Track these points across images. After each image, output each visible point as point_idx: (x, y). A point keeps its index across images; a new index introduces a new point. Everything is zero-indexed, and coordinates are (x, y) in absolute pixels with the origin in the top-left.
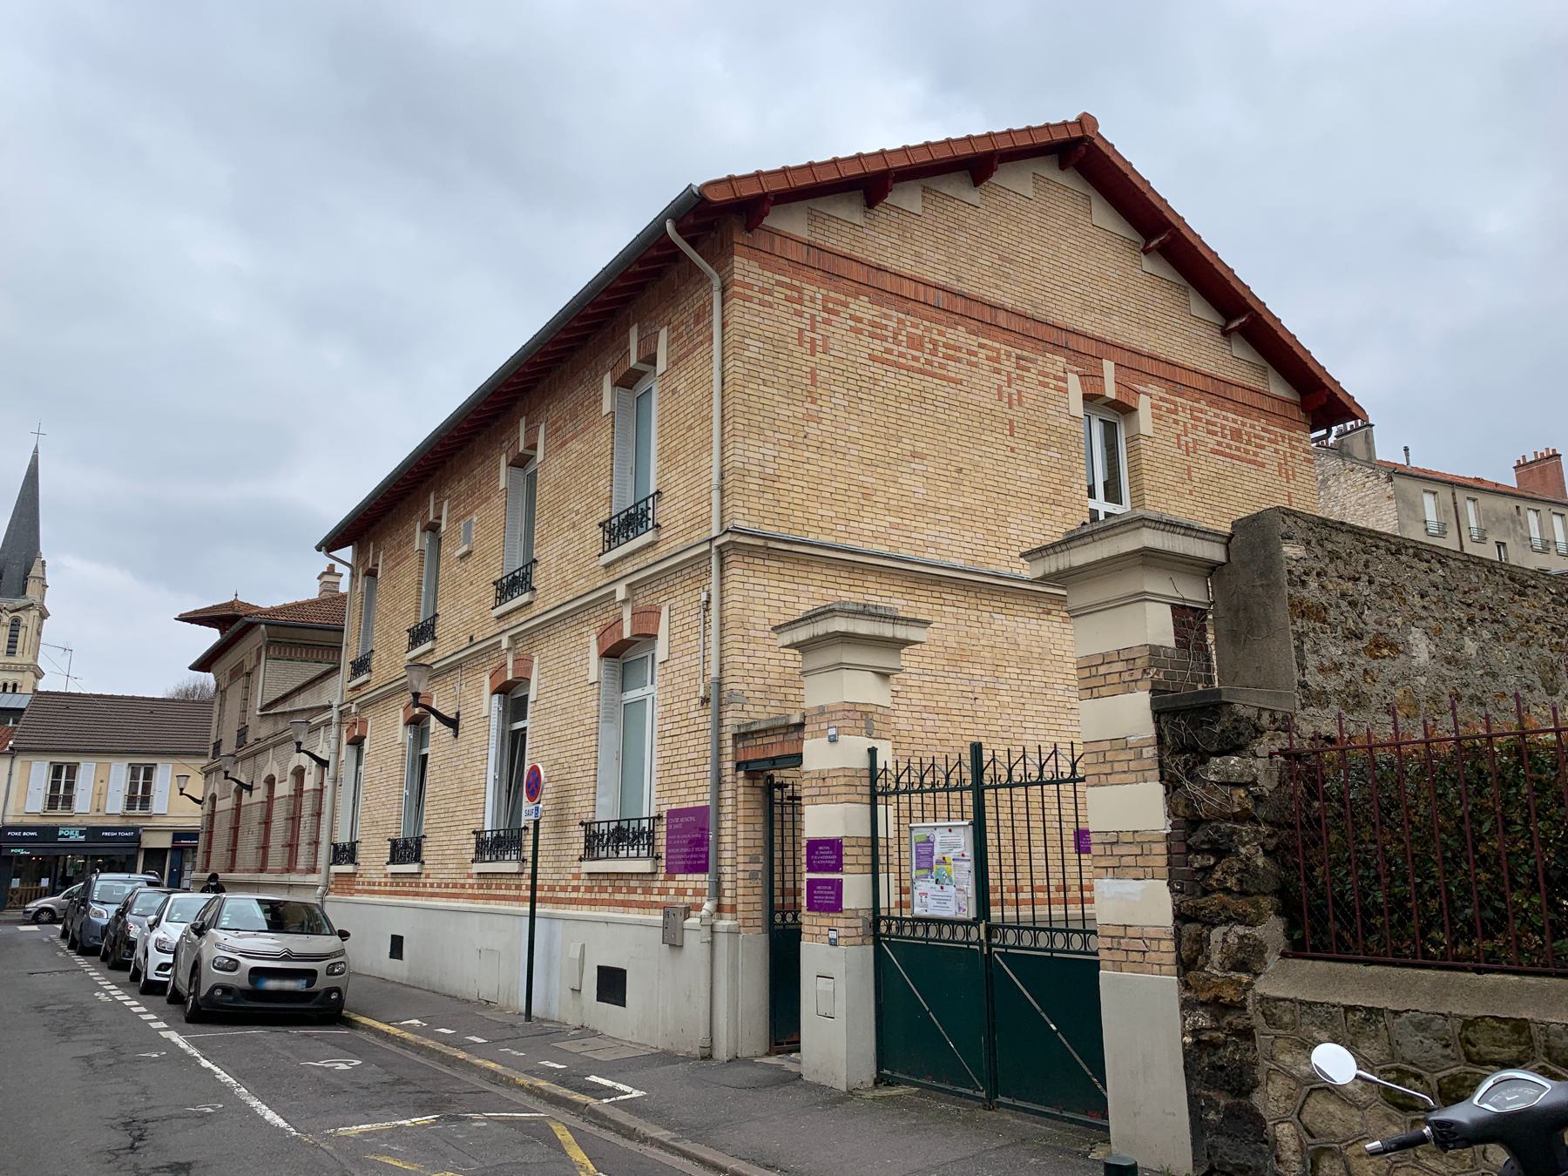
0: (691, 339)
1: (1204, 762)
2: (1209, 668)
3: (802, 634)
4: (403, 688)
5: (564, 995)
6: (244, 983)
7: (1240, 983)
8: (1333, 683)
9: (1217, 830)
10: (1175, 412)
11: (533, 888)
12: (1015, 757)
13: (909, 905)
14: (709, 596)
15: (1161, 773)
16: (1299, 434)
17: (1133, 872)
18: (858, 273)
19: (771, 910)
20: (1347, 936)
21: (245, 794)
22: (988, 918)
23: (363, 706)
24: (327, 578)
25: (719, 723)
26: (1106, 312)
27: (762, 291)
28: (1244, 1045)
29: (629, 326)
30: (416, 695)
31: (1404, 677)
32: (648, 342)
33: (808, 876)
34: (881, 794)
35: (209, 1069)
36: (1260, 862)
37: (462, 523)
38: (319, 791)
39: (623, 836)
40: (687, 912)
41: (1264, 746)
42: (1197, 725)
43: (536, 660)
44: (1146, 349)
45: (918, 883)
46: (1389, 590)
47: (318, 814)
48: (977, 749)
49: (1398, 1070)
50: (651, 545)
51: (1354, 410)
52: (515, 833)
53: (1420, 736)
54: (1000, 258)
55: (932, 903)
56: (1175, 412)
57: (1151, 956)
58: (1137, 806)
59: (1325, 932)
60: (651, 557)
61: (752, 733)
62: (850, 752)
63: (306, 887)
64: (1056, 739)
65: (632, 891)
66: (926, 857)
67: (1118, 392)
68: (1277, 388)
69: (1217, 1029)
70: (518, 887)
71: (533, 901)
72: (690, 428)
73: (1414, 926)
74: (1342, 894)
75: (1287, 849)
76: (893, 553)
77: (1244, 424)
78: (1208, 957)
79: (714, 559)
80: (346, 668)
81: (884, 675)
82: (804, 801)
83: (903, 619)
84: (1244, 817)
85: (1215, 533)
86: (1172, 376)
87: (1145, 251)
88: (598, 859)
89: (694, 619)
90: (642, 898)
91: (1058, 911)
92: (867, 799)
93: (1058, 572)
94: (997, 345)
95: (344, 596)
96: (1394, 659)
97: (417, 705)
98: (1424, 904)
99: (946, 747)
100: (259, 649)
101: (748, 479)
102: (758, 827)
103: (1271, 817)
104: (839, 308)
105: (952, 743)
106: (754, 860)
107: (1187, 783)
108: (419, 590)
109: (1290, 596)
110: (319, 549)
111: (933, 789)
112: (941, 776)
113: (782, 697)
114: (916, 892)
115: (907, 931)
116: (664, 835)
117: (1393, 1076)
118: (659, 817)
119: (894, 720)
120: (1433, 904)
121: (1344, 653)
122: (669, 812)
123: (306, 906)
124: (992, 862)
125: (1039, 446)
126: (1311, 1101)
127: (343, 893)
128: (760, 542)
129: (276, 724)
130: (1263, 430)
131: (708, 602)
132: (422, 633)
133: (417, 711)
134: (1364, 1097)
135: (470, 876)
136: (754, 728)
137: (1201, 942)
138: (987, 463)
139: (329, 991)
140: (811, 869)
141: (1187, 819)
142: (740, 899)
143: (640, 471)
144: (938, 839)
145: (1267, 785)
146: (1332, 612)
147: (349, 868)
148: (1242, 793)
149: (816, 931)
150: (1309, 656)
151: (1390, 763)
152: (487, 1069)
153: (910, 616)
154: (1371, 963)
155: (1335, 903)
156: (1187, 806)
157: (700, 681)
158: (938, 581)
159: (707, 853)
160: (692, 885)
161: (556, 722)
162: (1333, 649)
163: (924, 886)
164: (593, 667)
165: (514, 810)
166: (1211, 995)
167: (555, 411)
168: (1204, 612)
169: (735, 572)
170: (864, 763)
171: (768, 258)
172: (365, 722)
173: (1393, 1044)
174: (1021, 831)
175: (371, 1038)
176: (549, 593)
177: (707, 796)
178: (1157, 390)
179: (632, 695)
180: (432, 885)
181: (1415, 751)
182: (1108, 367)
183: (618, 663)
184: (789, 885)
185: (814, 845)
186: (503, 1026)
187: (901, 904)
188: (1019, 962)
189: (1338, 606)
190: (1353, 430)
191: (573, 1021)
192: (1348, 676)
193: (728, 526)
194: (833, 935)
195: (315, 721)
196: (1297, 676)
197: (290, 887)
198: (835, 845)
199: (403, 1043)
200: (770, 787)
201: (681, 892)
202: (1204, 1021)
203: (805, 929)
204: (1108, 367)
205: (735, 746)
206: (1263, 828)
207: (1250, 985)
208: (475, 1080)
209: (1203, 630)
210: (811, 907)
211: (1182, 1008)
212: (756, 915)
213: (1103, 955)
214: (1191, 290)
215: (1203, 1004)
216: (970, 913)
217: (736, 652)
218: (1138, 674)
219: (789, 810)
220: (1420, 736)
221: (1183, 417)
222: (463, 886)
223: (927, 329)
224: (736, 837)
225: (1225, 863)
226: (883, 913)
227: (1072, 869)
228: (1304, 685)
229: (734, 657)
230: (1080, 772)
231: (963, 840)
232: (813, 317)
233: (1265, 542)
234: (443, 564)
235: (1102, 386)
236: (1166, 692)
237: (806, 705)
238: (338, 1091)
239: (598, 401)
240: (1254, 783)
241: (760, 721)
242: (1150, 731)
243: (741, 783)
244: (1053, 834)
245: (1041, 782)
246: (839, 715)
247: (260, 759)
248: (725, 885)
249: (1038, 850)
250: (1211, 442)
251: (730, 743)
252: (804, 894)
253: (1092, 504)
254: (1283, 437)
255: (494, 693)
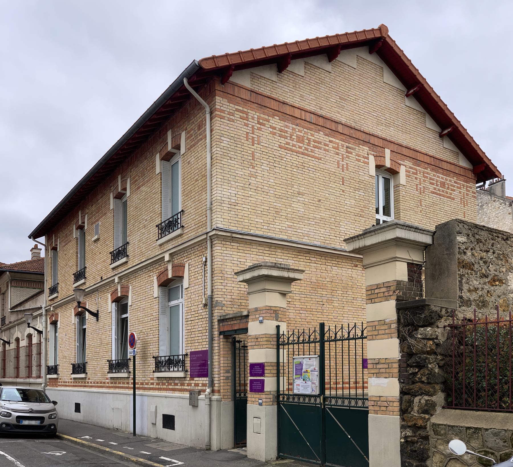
0: (196, 137)
1: (416, 330)
2: (421, 290)
3: (248, 276)
4: (73, 300)
5: (149, 426)
6: (15, 422)
7: (424, 418)
8: (474, 296)
9: (420, 357)
10: (416, 174)
11: (134, 383)
12: (311, 332)
13: (292, 390)
14: (206, 259)
15: (398, 334)
16: (471, 184)
17: (384, 375)
18: (274, 105)
19: (235, 392)
20: (470, 400)
21: (7, 346)
22: (324, 394)
23: (56, 308)
24: (34, 251)
25: (211, 315)
26: (388, 125)
27: (229, 113)
28: (425, 442)
29: (167, 131)
30: (79, 303)
31: (504, 294)
32: (176, 138)
33: (250, 378)
34: (281, 344)
35: (3, 455)
36: (437, 371)
37: (94, 225)
38: (39, 344)
39: (171, 362)
40: (199, 392)
41: (442, 323)
42: (414, 314)
43: (130, 287)
44: (405, 144)
45: (296, 381)
46: (501, 257)
47: (39, 354)
48: (322, 325)
49: (485, 451)
50: (180, 235)
51: (497, 173)
52: (125, 361)
53: (508, 319)
54: (340, 98)
55: (301, 388)
56: (416, 174)
57: (390, 408)
58: (388, 349)
59: (461, 399)
60: (180, 241)
61: (226, 319)
62: (269, 327)
63: (37, 383)
64: (356, 322)
65: (176, 384)
66: (299, 370)
67: (391, 164)
68: (463, 163)
69: (414, 436)
70: (128, 383)
71: (134, 389)
72: (197, 180)
73: (497, 396)
74: (469, 383)
75: (448, 366)
76: (289, 239)
77: (446, 180)
78: (413, 409)
79: (209, 242)
80: (47, 291)
81: (283, 294)
82: (248, 348)
83: (293, 269)
84: (432, 352)
85: (428, 231)
86: (415, 157)
87: (407, 96)
88: (161, 372)
89: (199, 268)
90: (180, 387)
91: (353, 392)
92: (275, 347)
93: (360, 248)
94: (337, 141)
95: (43, 259)
96: (501, 286)
97: (80, 307)
98: (502, 387)
99: (310, 325)
100: (8, 282)
101: (223, 205)
102: (229, 359)
103: (443, 352)
104: (265, 122)
105: (312, 323)
106: (227, 372)
107: (409, 339)
108: (77, 256)
109: (459, 259)
110: (30, 237)
111: (303, 342)
112: (307, 337)
113: (239, 304)
114: (295, 384)
115: (291, 400)
116: (189, 362)
117: (483, 453)
118: (187, 355)
119: (287, 314)
120: (506, 387)
121: (480, 284)
122: (191, 352)
123: (37, 391)
124: (327, 372)
125: (355, 189)
126: (450, 463)
127: (53, 386)
128: (229, 234)
129: (17, 315)
130: (455, 182)
131: (206, 262)
132: (80, 275)
133: (80, 309)
134: (471, 462)
135: (107, 379)
136: (227, 317)
137: (410, 403)
138: (332, 197)
139: (50, 425)
140: (251, 375)
141: (408, 354)
142: (222, 388)
143: (174, 200)
144: (305, 363)
145: (442, 339)
146: (476, 266)
147: (55, 376)
148: (431, 342)
149: (254, 400)
150: (464, 285)
151: (494, 330)
152: (118, 455)
153: (297, 268)
154: (478, 410)
155: (466, 387)
156: (408, 348)
157: (203, 296)
158: (309, 252)
159: (207, 369)
160: (201, 382)
161: (140, 314)
162: (475, 282)
163: (299, 382)
164: (156, 291)
165: (124, 352)
166: (413, 423)
167: (134, 172)
168: (421, 266)
169: (218, 248)
170: (274, 331)
171: (232, 97)
172: (57, 314)
173: (484, 442)
174: (339, 360)
175: (69, 443)
176: (136, 257)
177: (207, 346)
178: (408, 163)
179: (173, 303)
180: (91, 383)
181: (505, 325)
182: (388, 152)
183: (166, 289)
184: (242, 382)
185: (253, 366)
186: (124, 438)
187: (288, 389)
188: (336, 411)
189: (479, 263)
190: (497, 182)
191: (153, 436)
192: (480, 293)
193: (214, 227)
194: (260, 401)
195: (35, 314)
196: (459, 293)
197: (30, 384)
198: (261, 366)
199: (83, 445)
200: (234, 342)
201: (197, 385)
202: (409, 433)
203: (249, 399)
204: (388, 152)
205: (219, 325)
206: (439, 357)
207: (429, 419)
208: (113, 459)
209: (420, 274)
210: (251, 390)
211: (401, 428)
212: (229, 394)
213: (370, 408)
214: (427, 116)
215: (409, 427)
216: (317, 392)
217: (218, 284)
218: (391, 293)
219: (242, 351)
220: (508, 319)
221: (420, 176)
222: (104, 383)
223: (306, 133)
224: (220, 362)
225: (422, 371)
226: (281, 393)
227: (360, 375)
228: (461, 297)
229: (218, 286)
230: (365, 335)
231: (315, 363)
232: (253, 126)
233: (449, 235)
234: (87, 244)
235: (384, 161)
236: (403, 300)
237: (249, 307)
238: (57, 463)
239: (154, 167)
240: (437, 338)
241: (229, 314)
242: (395, 317)
243: (221, 340)
244: (353, 360)
245: (349, 339)
246: (264, 312)
247: (12, 331)
248: (215, 382)
249: (346, 368)
250: (431, 188)
251: (216, 323)
252: (249, 385)
253: (378, 216)
254: (464, 186)
255: (113, 302)
